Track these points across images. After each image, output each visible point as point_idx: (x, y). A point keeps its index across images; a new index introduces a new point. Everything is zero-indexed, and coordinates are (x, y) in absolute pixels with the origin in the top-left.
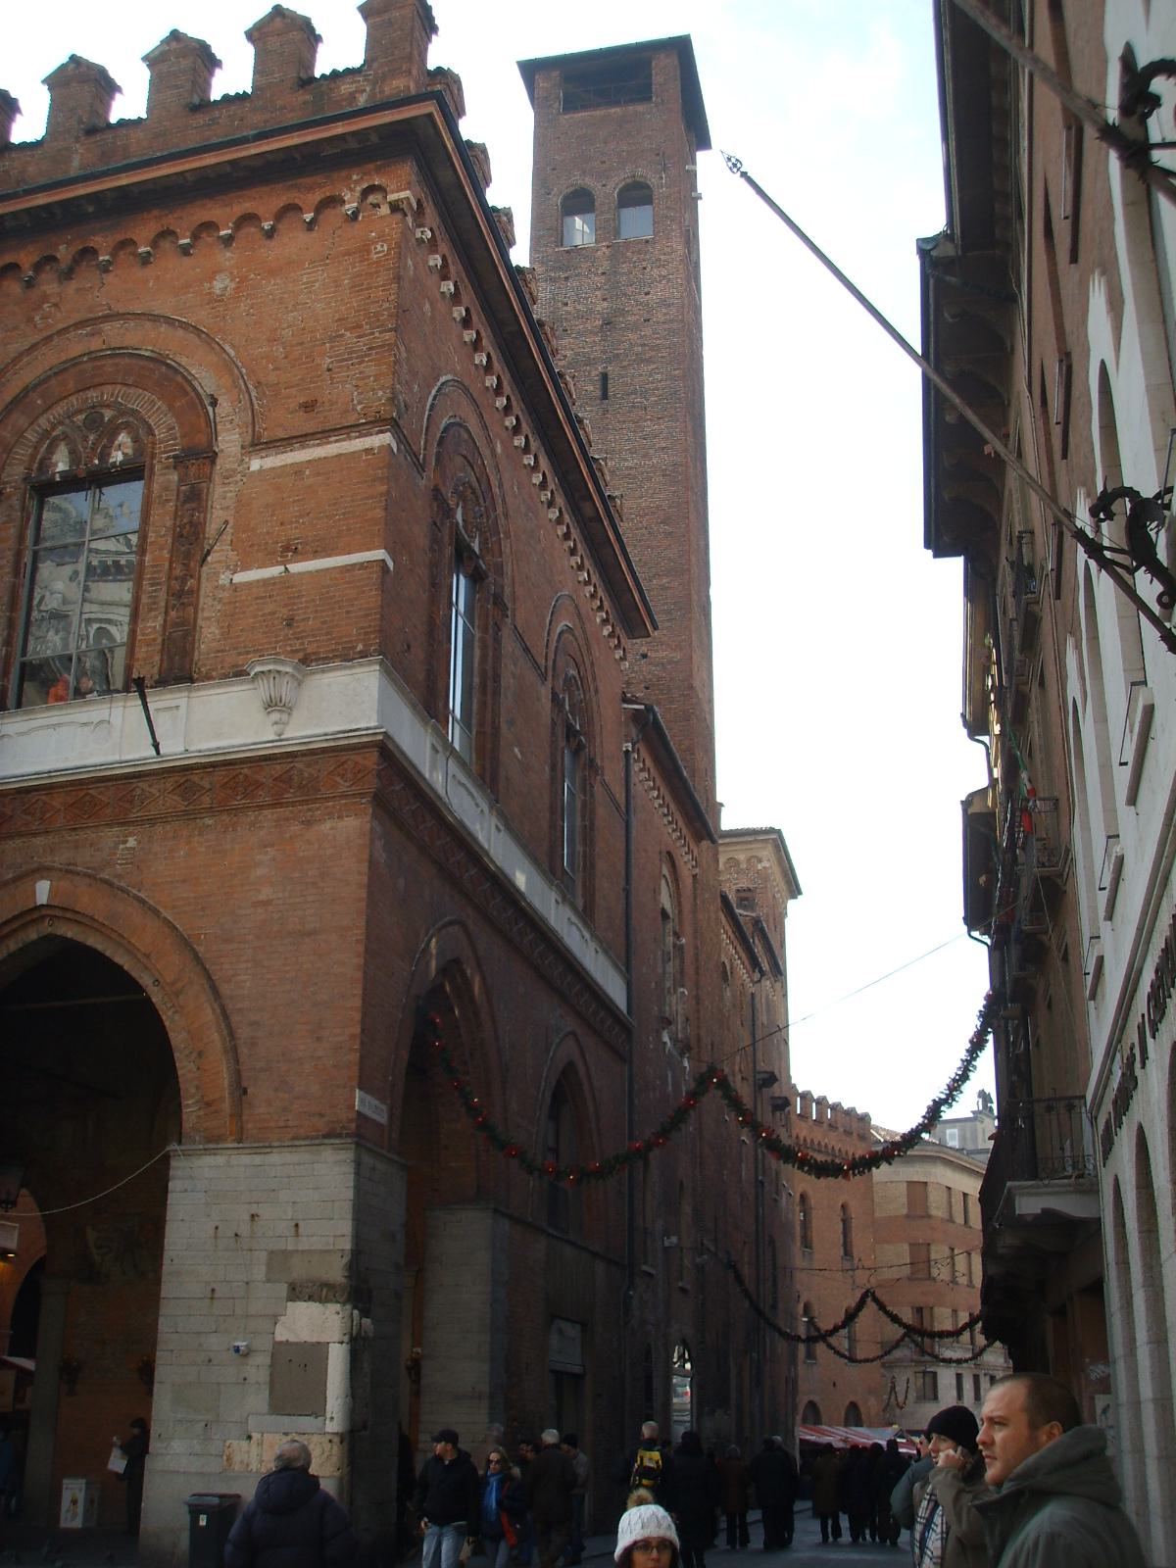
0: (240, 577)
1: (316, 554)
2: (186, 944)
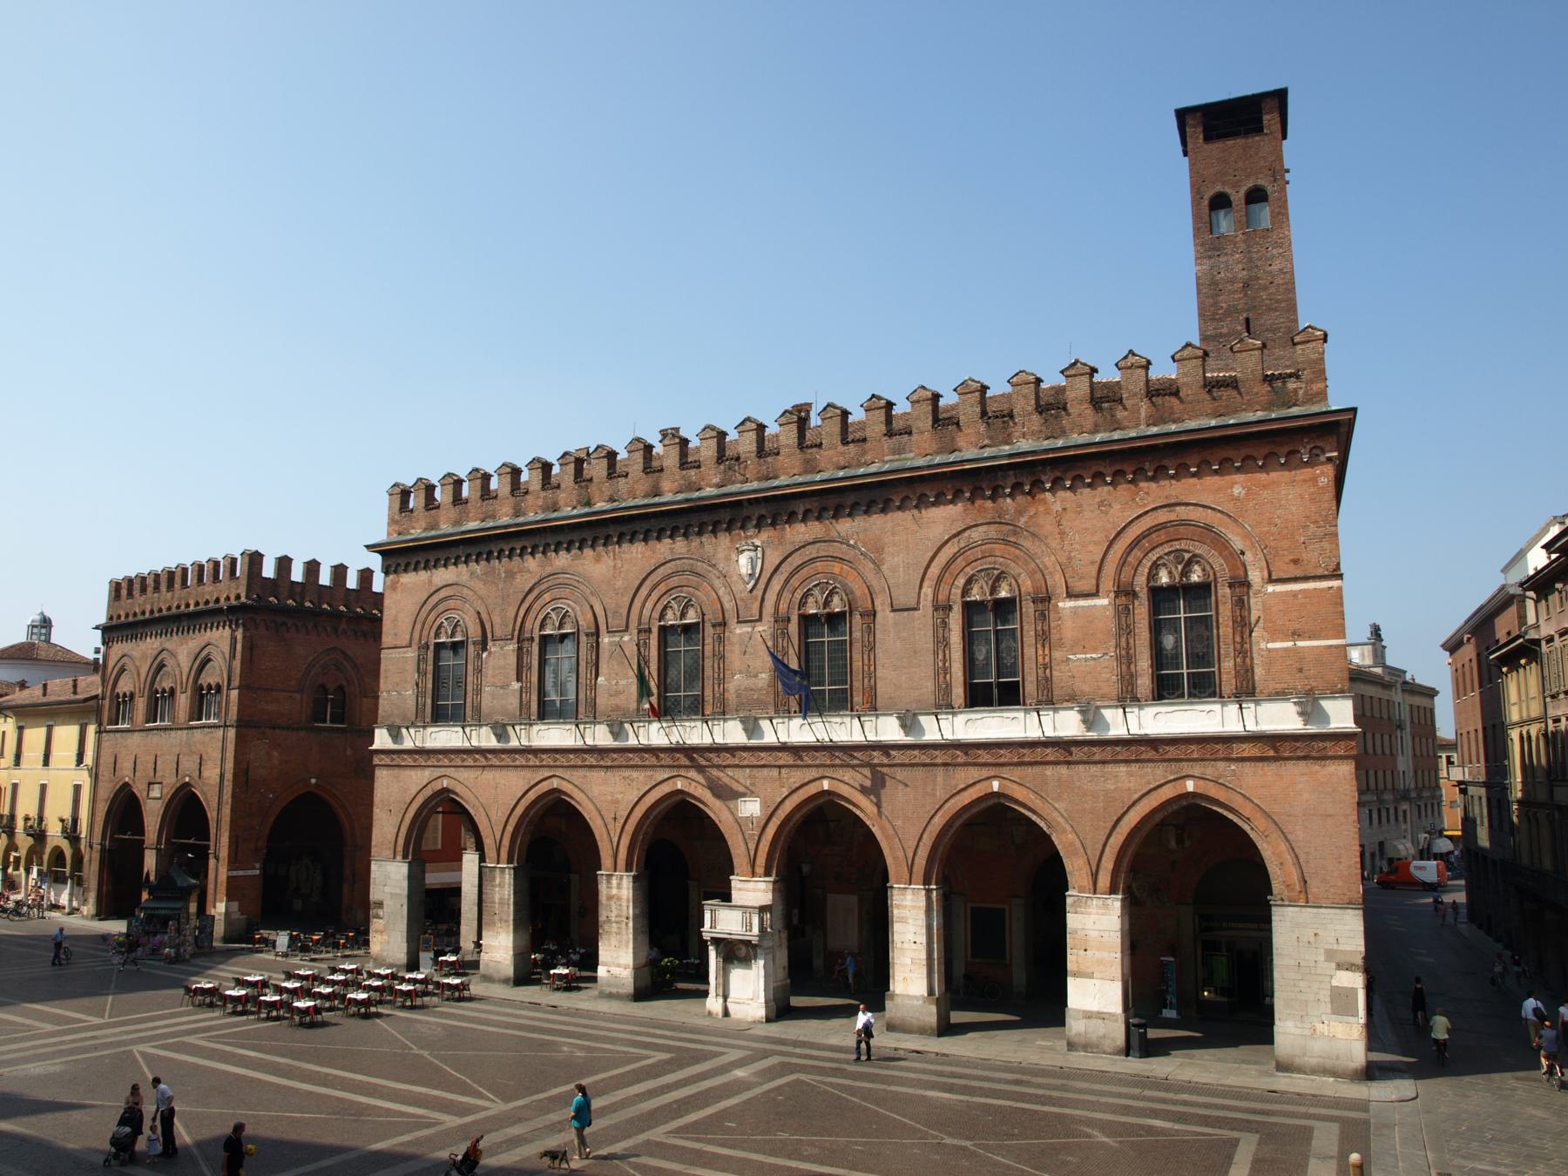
0: (1270, 645)
1: (1310, 638)
2: (1267, 815)
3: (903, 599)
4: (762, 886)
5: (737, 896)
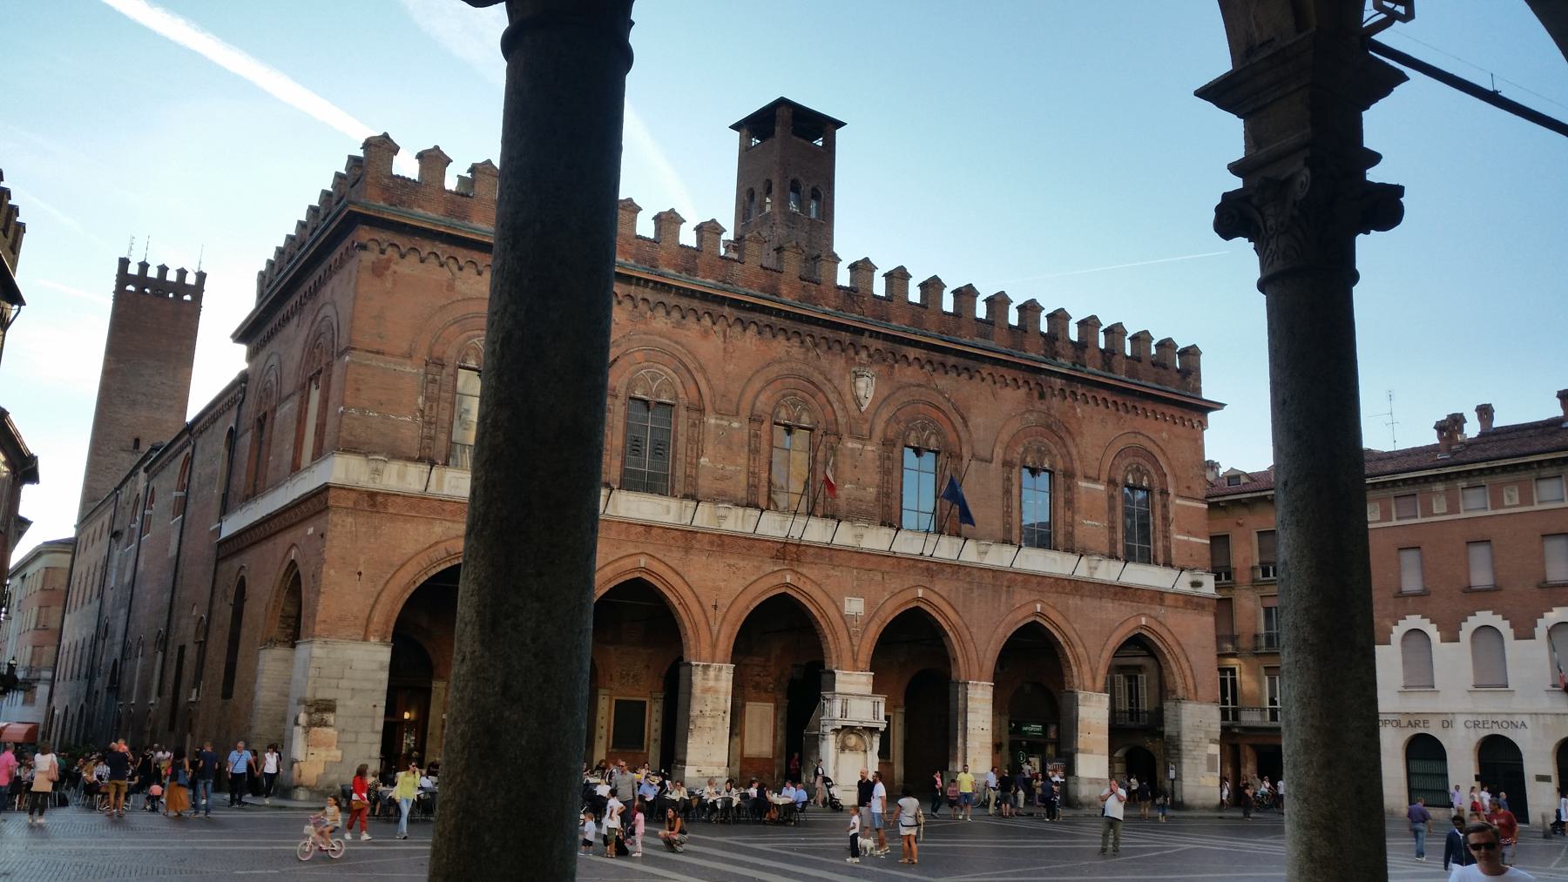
2: (1179, 644)
3: (983, 451)
5: (839, 688)
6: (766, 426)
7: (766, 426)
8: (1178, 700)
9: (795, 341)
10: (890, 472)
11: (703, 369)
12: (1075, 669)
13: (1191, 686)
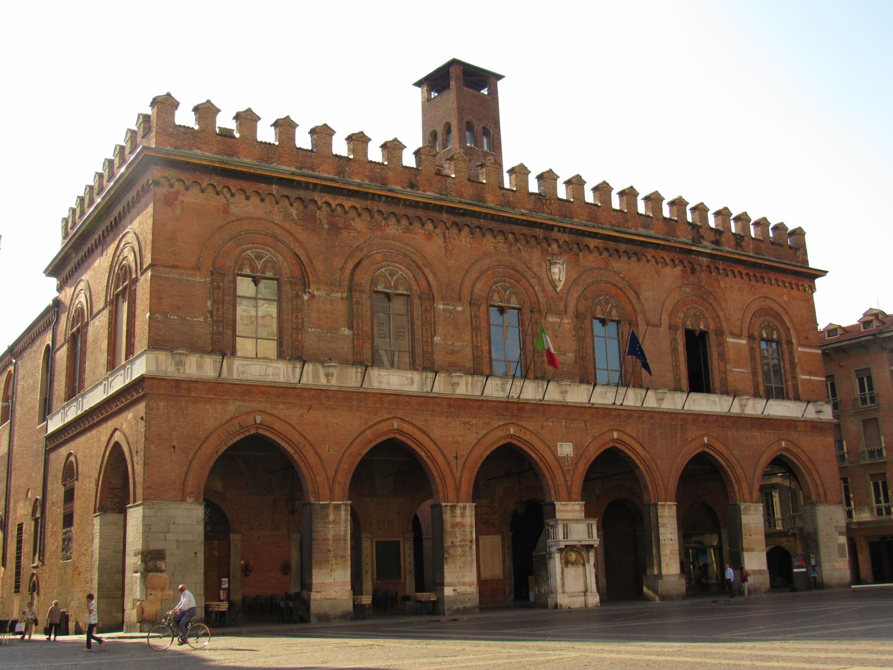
2: (811, 460)
4: (577, 508)
5: (558, 515)
6: (483, 307)
7: (483, 307)
8: (813, 504)
9: (500, 238)
10: (583, 338)
11: (429, 265)
12: (736, 486)
13: (821, 492)
